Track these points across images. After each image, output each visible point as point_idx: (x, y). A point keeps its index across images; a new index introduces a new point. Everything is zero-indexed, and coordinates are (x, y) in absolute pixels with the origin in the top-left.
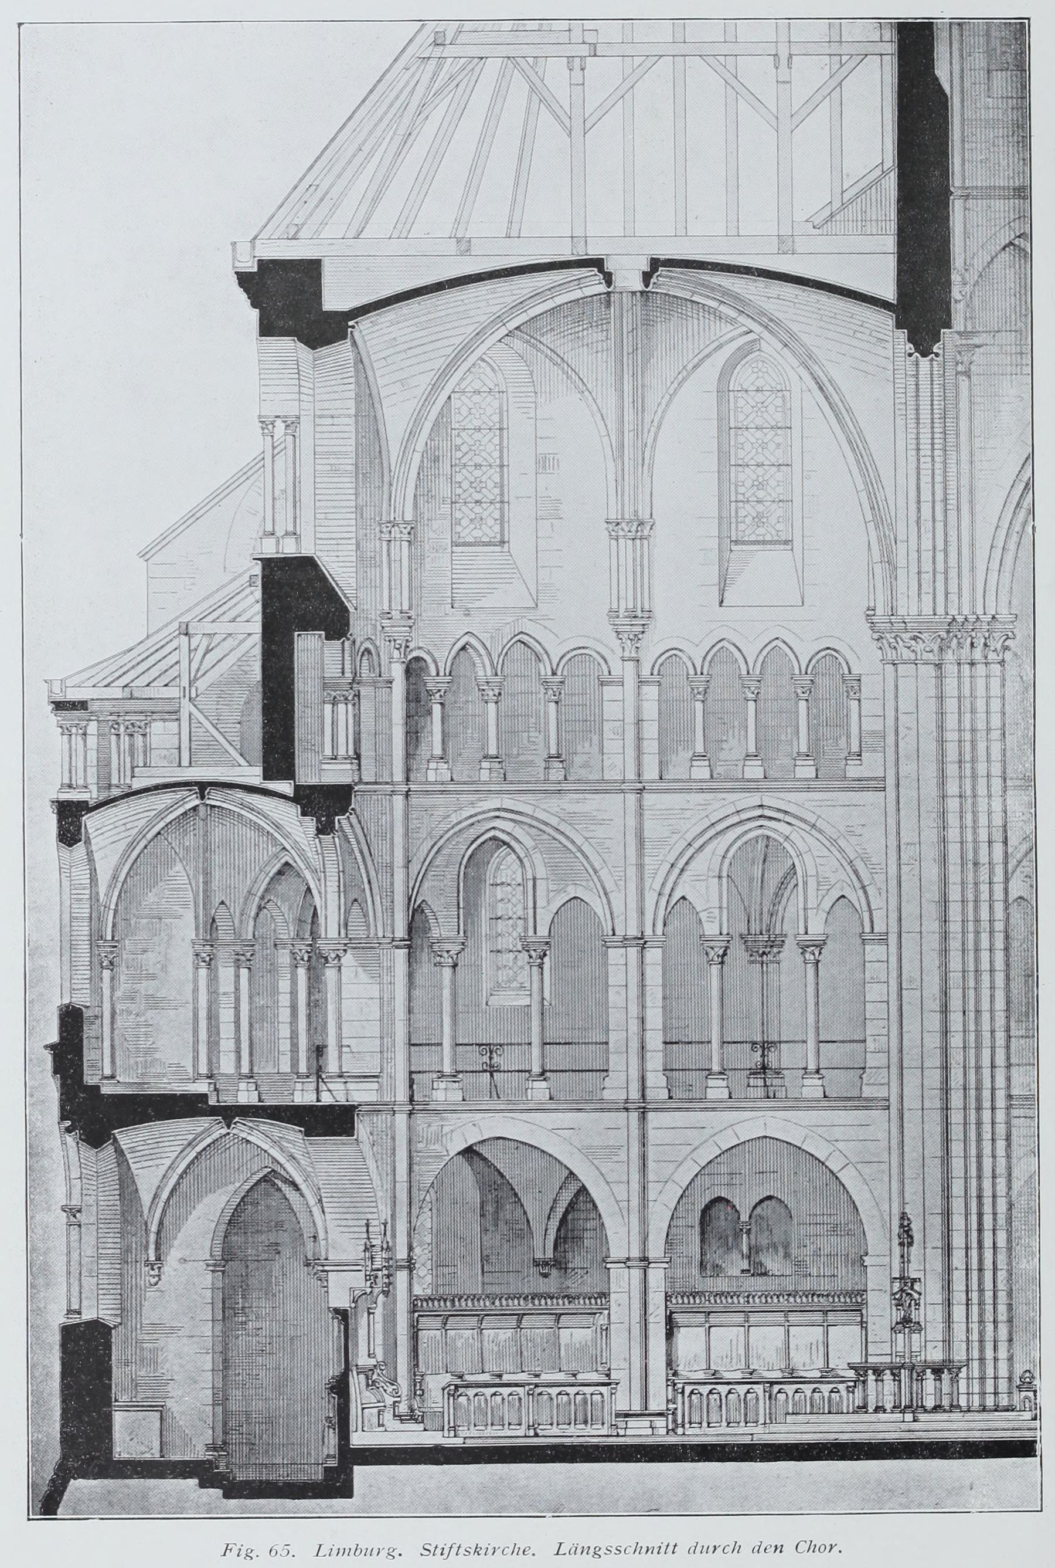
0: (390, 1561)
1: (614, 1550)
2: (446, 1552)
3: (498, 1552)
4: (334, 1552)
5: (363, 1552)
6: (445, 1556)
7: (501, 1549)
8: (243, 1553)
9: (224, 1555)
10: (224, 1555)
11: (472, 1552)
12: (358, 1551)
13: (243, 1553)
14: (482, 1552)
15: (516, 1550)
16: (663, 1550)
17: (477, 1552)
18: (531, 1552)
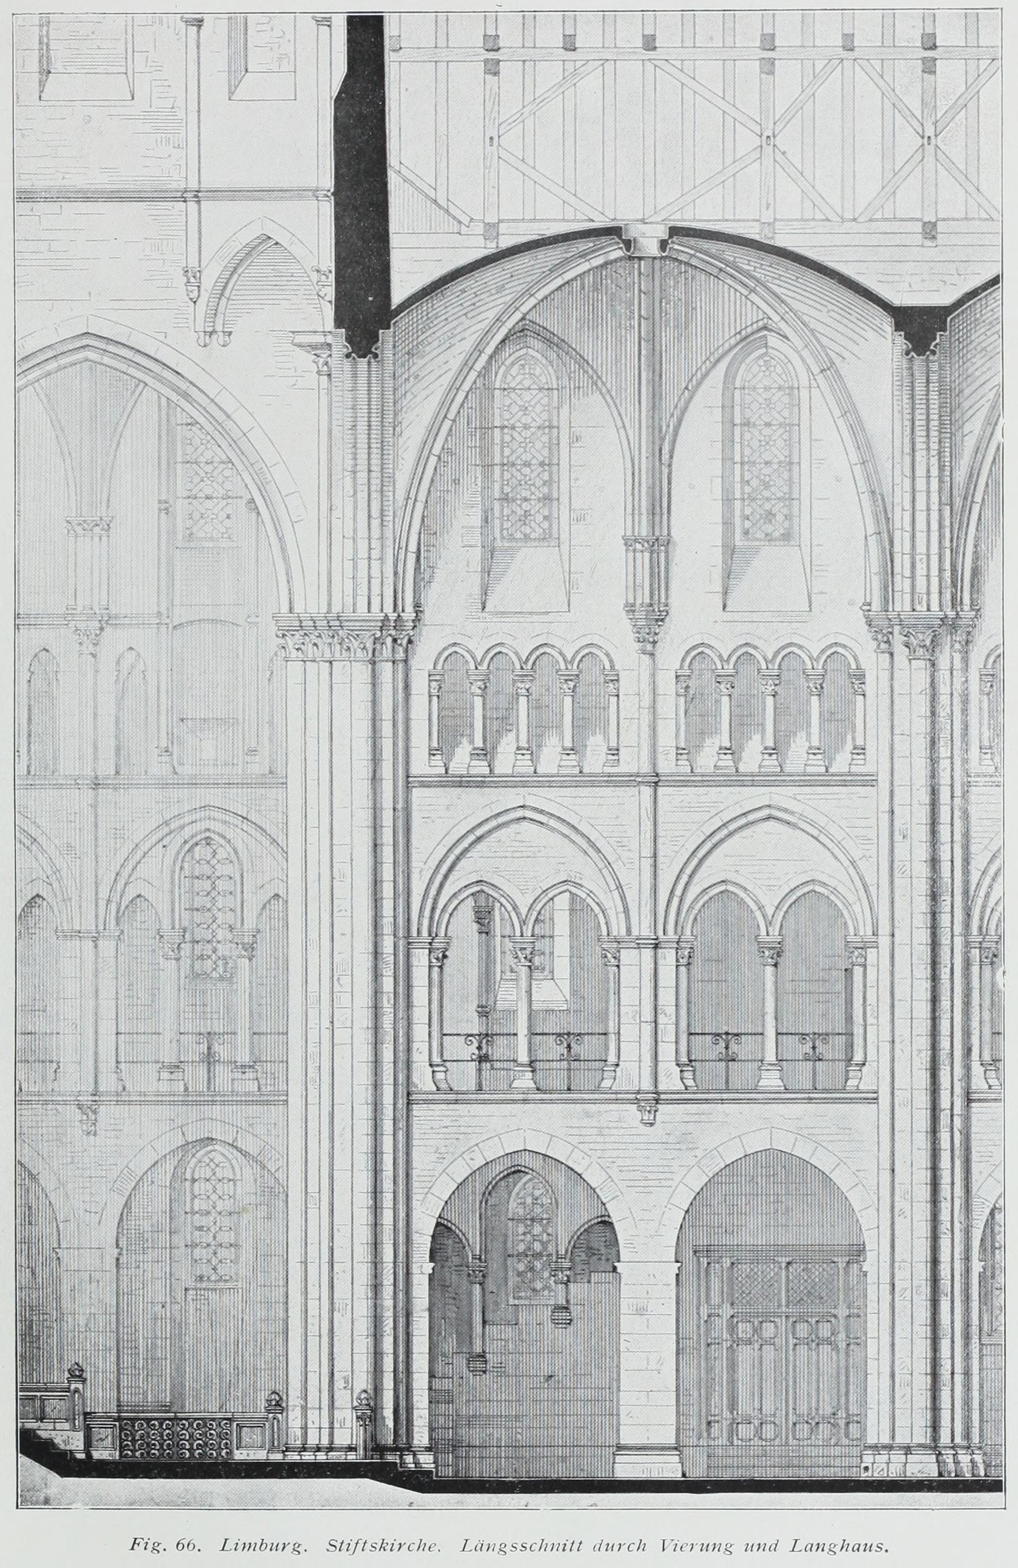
0: (295, 1556)
1: (519, 1547)
2: (352, 1547)
3: (405, 1548)
4: (240, 1547)
5: (269, 1547)
6: (351, 1552)
7: (407, 1546)
8: (150, 1547)
9: (132, 1549)
10: (132, 1549)
11: (378, 1547)
12: (264, 1546)
13: (150, 1547)
14: (389, 1547)
15: (421, 1546)
16: (568, 1548)
17: (382, 1548)
18: (436, 1549)
